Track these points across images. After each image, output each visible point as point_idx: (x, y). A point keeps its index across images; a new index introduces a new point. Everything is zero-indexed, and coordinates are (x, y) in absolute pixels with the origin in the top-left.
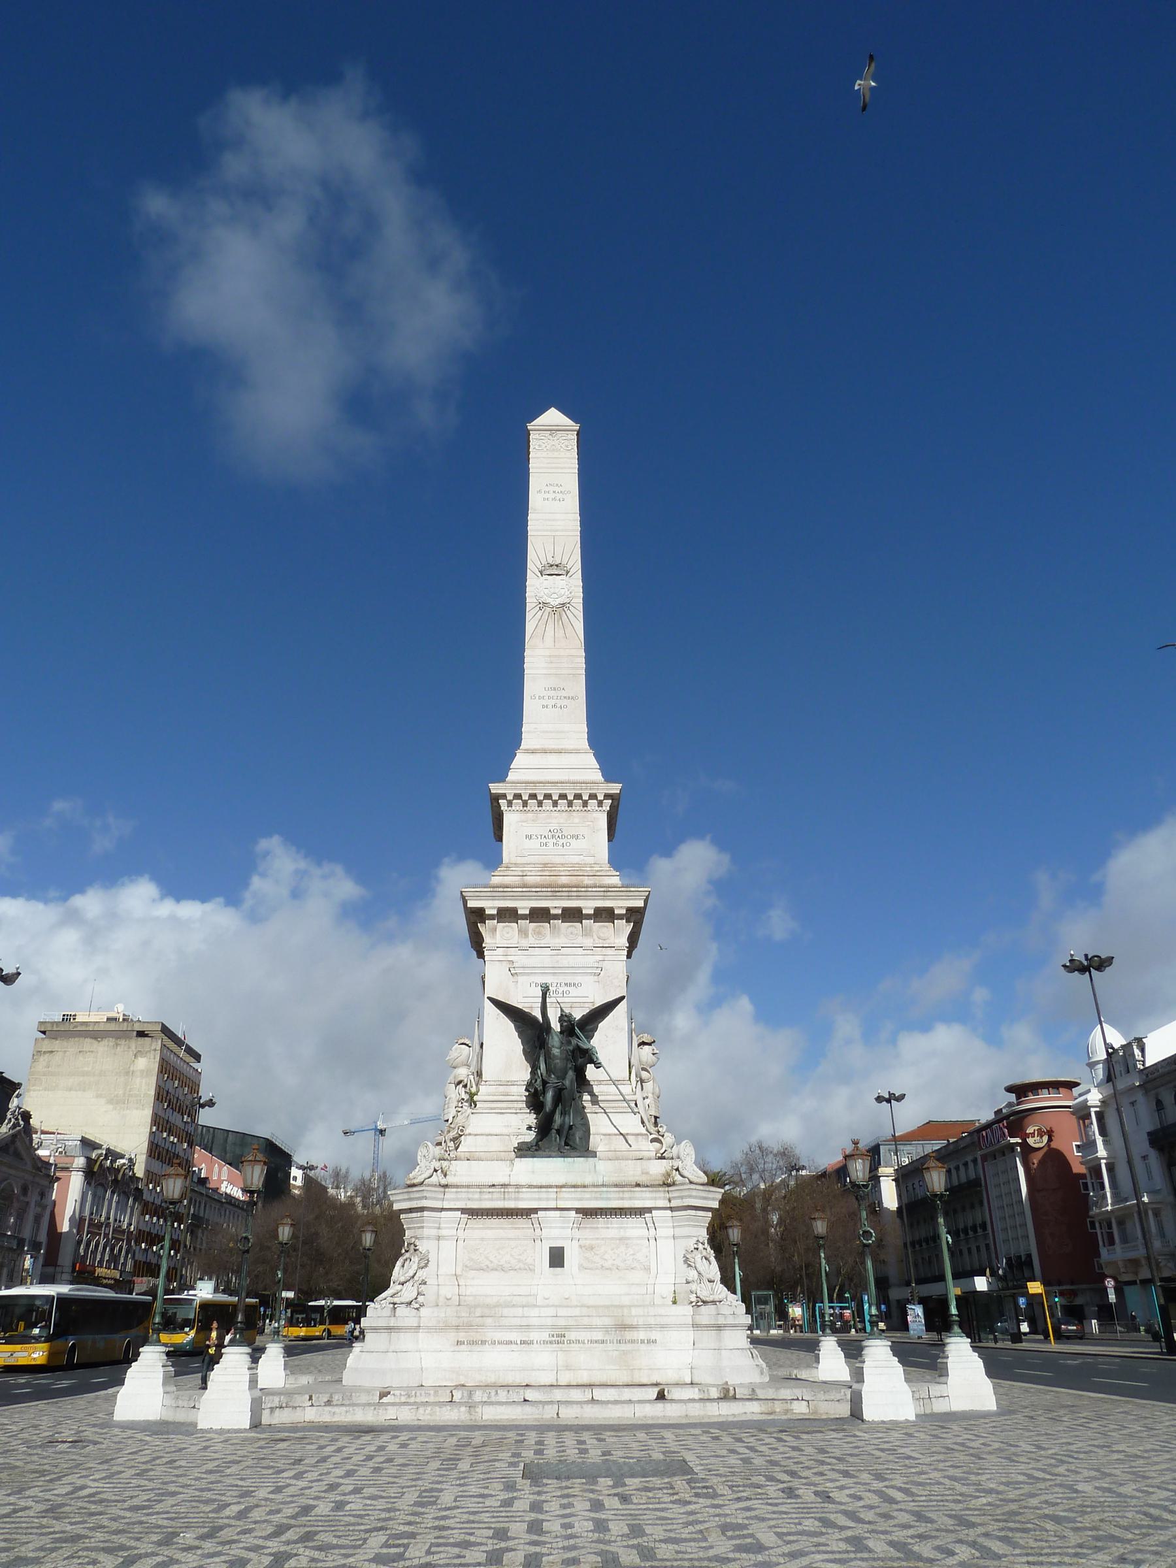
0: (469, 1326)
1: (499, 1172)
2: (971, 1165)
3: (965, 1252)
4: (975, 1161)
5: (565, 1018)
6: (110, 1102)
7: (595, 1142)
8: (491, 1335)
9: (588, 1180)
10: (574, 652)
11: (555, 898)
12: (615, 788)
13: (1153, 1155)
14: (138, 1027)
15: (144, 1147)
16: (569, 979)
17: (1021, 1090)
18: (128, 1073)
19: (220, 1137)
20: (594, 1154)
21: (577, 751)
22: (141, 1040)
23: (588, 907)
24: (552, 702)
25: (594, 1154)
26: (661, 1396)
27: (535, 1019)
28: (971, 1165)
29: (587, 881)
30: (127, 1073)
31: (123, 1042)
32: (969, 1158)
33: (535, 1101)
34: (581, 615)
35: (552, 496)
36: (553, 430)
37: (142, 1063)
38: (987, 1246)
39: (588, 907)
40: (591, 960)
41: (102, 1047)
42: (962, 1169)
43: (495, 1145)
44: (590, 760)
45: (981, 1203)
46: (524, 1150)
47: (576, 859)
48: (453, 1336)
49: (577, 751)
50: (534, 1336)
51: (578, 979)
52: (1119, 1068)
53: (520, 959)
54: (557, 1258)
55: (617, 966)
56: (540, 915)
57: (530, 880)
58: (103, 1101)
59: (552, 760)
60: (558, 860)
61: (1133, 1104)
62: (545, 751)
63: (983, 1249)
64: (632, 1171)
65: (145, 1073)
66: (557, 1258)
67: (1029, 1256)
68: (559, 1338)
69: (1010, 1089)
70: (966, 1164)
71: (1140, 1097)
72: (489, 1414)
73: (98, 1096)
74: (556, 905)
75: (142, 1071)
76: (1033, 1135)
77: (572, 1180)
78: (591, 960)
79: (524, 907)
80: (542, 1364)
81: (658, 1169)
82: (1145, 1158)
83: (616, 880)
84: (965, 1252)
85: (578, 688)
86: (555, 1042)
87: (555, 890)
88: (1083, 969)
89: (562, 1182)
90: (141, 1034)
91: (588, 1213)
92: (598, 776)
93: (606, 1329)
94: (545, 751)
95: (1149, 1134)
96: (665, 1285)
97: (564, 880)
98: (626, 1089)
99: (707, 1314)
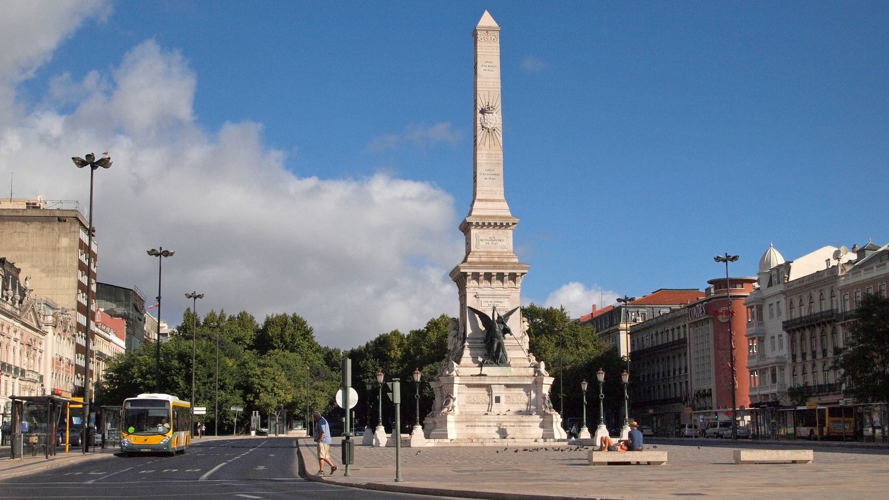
0: (471, 421)
2: (682, 329)
3: (672, 386)
4: (685, 326)
5: (499, 317)
6: (43, 271)
8: (477, 424)
9: (508, 374)
10: (498, 152)
11: (494, 268)
12: (516, 220)
13: (785, 334)
14: (58, 214)
15: (74, 305)
16: (499, 300)
17: (719, 284)
18: (55, 249)
19: (273, 332)
20: (509, 365)
21: (500, 201)
22: (62, 224)
24: (488, 177)
25: (509, 365)
26: (536, 441)
27: (488, 317)
28: (682, 329)
29: (505, 260)
30: (54, 249)
31: (47, 225)
32: (681, 324)
34: (501, 133)
35: (487, 68)
36: (488, 30)
37: (65, 242)
38: (687, 382)
39: (506, 272)
40: (506, 292)
41: (32, 229)
42: (676, 331)
44: (505, 205)
45: (685, 354)
47: (500, 250)
48: (466, 424)
49: (500, 201)
50: (491, 424)
51: (502, 300)
52: (775, 279)
53: (480, 292)
54: (498, 400)
55: (516, 295)
57: (483, 259)
58: (37, 270)
59: (490, 205)
60: (493, 250)
61: (778, 302)
62: (486, 200)
63: (684, 384)
65: (69, 249)
67: (710, 390)
69: (710, 282)
70: (679, 328)
71: (782, 299)
72: (487, 444)
73: (34, 267)
74: (494, 272)
75: (66, 248)
76: (722, 314)
77: (502, 374)
78: (506, 292)
79: (482, 272)
82: (780, 336)
83: (516, 260)
84: (672, 386)
85: (500, 170)
87: (495, 265)
88: (725, 261)
89: (499, 374)
90: (60, 220)
91: (508, 386)
92: (509, 214)
93: (515, 422)
94: (486, 200)
95: (784, 323)
97: (496, 260)
98: (520, 341)
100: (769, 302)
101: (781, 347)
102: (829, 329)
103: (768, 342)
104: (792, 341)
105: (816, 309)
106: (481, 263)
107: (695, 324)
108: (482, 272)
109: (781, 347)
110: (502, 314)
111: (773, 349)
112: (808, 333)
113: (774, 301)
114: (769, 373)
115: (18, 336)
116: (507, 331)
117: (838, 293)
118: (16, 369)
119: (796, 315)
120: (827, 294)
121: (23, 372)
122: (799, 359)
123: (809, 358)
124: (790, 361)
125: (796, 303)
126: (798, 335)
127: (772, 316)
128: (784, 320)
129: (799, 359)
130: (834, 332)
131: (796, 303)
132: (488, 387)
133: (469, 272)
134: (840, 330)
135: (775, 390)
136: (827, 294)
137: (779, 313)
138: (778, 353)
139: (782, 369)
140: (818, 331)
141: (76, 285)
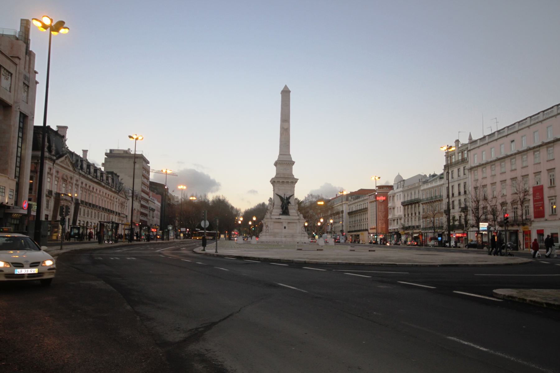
1: (278, 217)
7: (291, 214)
13: (402, 207)
15: (140, 190)
23: (290, 181)
33: (282, 208)
39: (290, 181)
43: (277, 214)
46: (280, 215)
54: (285, 228)
56: (283, 182)
57: (282, 176)
64: (295, 218)
66: (285, 228)
68: (285, 237)
71: (401, 193)
74: (285, 181)
80: (284, 239)
81: (298, 217)
86: (285, 201)
91: (289, 223)
96: (298, 231)
99: (303, 235)
100: (397, 194)
101: (400, 211)
102: (417, 205)
103: (396, 209)
104: (405, 209)
105: (413, 198)
106: (281, 177)
107: (371, 202)
108: (281, 181)
109: (400, 211)
110: (288, 196)
111: (398, 212)
112: (410, 206)
113: (398, 194)
114: (396, 221)
115: (117, 200)
116: (289, 203)
117: (421, 192)
118: (116, 212)
119: (406, 200)
120: (417, 192)
121: (119, 214)
122: (407, 216)
123: (410, 216)
124: (403, 216)
125: (406, 195)
126: (406, 207)
127: (398, 200)
128: (402, 200)
129: (407, 216)
130: (419, 206)
131: (406, 195)
132: (282, 222)
133: (276, 181)
134: (421, 205)
135: (397, 227)
136: (417, 192)
137: (400, 199)
138: (399, 214)
139: (400, 219)
140: (413, 206)
141: (141, 182)
